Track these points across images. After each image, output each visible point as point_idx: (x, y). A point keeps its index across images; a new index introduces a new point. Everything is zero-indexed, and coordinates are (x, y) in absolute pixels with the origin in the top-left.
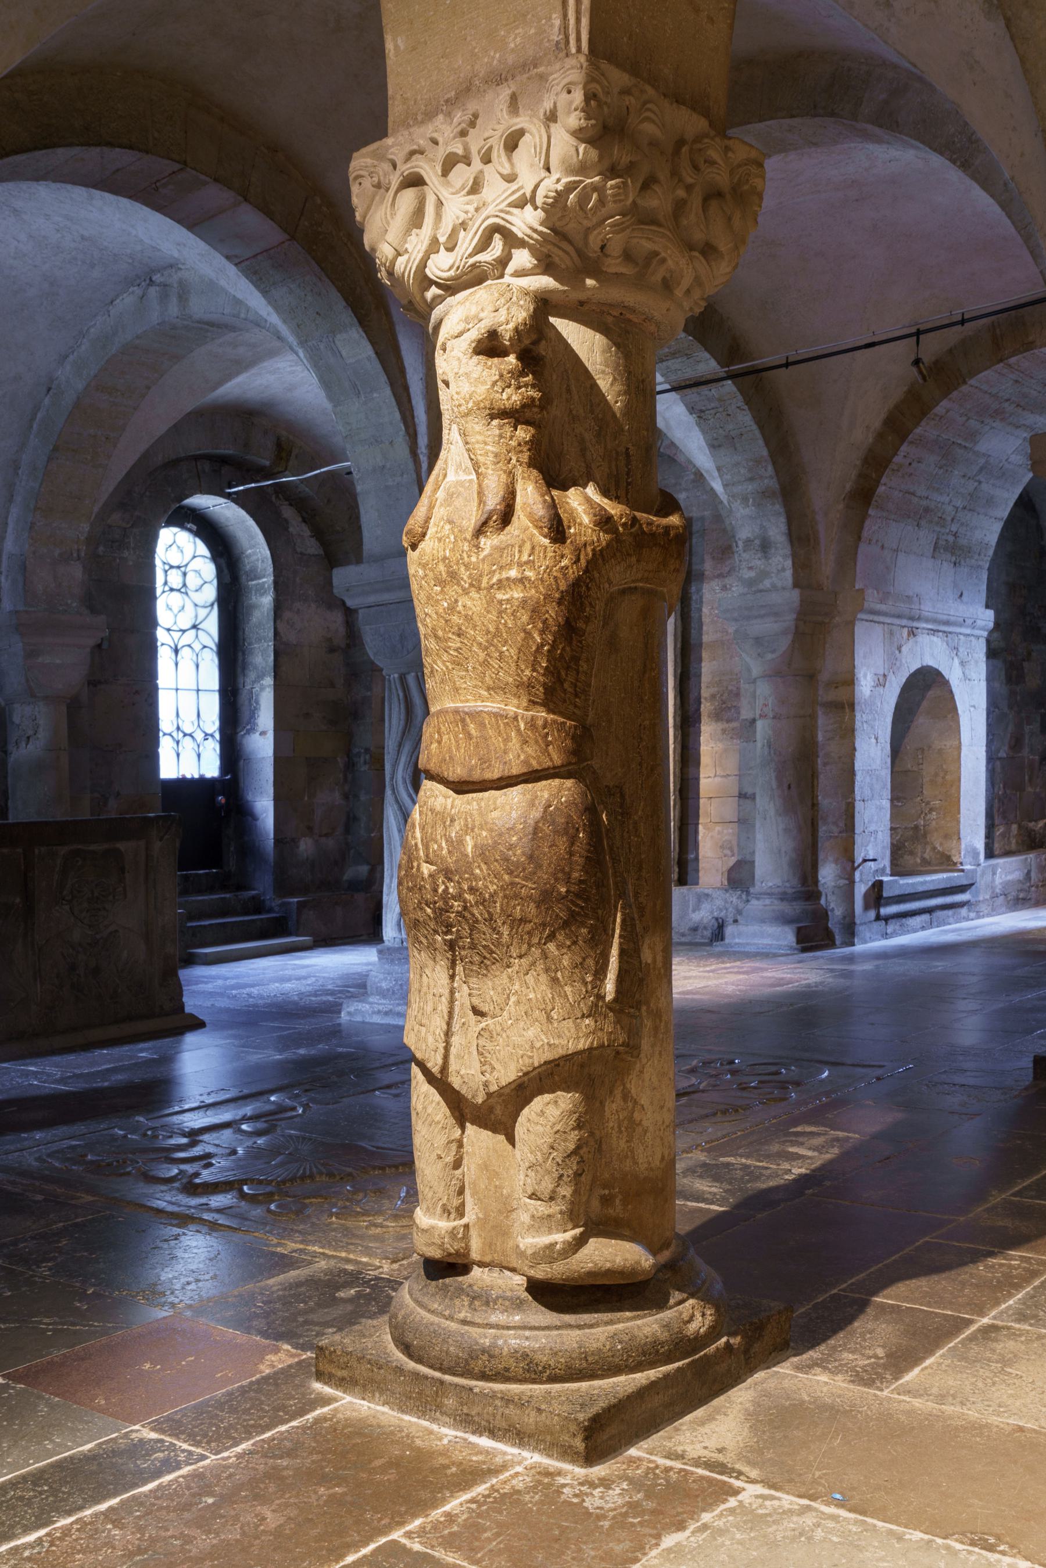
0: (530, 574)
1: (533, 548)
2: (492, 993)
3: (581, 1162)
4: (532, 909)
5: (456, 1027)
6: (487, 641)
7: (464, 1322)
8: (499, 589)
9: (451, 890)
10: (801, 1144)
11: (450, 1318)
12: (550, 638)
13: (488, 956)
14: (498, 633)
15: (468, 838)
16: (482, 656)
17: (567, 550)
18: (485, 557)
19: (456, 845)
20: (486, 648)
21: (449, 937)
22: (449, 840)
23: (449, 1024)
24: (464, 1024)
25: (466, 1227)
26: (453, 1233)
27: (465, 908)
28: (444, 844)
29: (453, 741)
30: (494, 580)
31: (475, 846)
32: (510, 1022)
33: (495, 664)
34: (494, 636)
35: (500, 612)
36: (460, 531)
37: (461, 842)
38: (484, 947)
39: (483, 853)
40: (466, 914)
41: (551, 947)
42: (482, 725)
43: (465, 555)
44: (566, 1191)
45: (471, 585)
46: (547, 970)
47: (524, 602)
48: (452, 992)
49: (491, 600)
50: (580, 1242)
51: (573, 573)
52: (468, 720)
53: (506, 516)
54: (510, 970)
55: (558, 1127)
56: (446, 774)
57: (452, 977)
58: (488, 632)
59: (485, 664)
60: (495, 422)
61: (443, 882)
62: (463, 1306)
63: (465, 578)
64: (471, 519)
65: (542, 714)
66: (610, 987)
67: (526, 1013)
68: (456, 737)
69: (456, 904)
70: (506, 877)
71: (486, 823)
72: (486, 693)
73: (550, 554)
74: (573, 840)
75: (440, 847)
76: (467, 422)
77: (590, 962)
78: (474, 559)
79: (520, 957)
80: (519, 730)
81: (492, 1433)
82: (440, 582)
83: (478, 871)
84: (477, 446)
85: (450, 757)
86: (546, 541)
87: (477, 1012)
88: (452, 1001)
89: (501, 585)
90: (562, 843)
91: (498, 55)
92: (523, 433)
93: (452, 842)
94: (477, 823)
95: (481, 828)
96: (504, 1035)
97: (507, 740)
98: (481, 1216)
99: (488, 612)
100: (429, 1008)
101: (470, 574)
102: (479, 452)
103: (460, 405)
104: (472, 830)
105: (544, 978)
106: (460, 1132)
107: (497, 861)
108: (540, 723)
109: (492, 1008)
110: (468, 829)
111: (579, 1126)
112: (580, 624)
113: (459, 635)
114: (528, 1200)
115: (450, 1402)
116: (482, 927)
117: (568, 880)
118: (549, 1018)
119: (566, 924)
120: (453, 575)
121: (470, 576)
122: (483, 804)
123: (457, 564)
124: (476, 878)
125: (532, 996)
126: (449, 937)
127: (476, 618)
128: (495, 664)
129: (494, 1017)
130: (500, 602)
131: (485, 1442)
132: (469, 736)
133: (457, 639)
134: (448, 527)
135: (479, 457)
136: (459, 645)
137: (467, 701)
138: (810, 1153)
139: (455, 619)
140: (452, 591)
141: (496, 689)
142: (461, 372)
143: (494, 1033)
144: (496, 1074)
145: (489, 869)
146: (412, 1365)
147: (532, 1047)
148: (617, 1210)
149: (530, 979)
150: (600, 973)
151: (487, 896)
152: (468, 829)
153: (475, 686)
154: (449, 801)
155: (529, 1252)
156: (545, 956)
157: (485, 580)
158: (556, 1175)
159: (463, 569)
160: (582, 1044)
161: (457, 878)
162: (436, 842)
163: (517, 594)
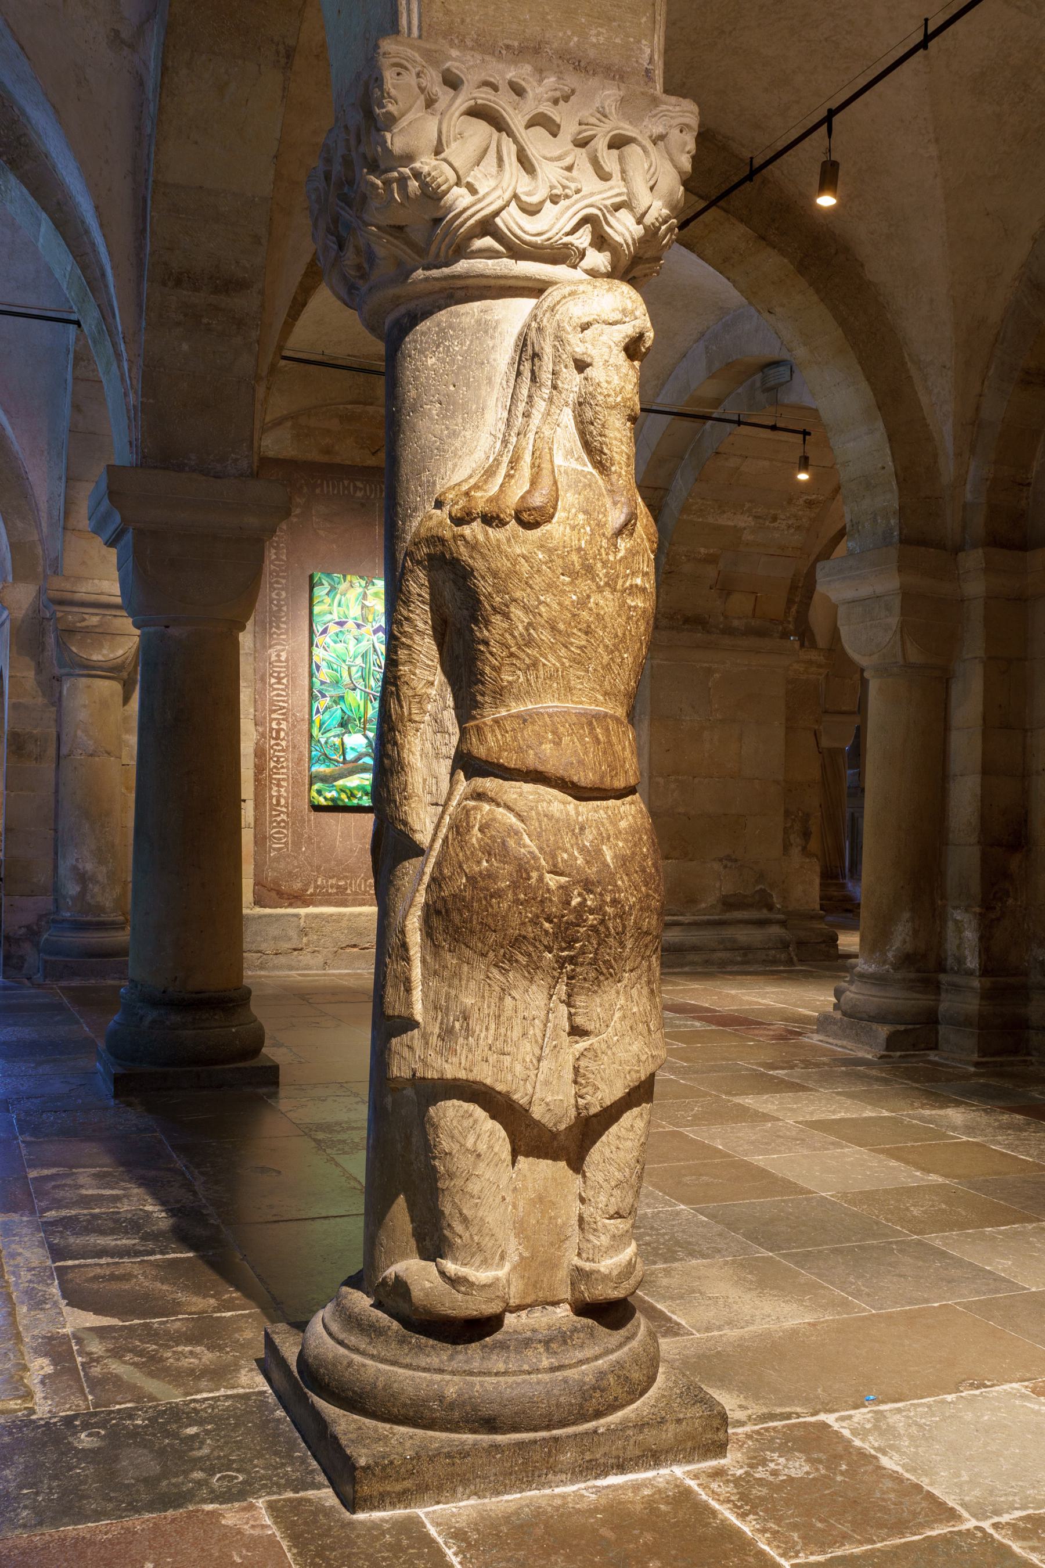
2: (599, 1010)
6: (614, 645)
7: (553, 1369)
8: (629, 594)
9: (589, 903)
11: (538, 1371)
13: (605, 971)
15: (604, 847)
16: (606, 659)
18: (622, 558)
19: (593, 855)
20: (612, 652)
22: (582, 850)
24: (555, 1047)
27: (602, 922)
28: (576, 853)
29: (577, 744)
30: (628, 584)
31: (615, 856)
32: (615, 1038)
34: (621, 641)
36: (598, 525)
37: (599, 852)
38: (604, 962)
40: (602, 929)
43: (603, 550)
45: (607, 584)
54: (619, 985)
56: (575, 779)
58: (616, 636)
59: (607, 668)
61: (580, 895)
63: (601, 575)
67: (631, 1028)
69: (591, 917)
70: (643, 889)
71: (620, 832)
72: (601, 698)
76: (610, 415)
79: (631, 971)
81: (621, 1468)
82: (574, 575)
83: (619, 883)
84: (614, 442)
85: (579, 762)
91: (576, 39)
93: (589, 851)
94: (611, 833)
95: (617, 838)
96: (609, 1052)
98: (526, 1254)
99: (619, 616)
101: (608, 573)
102: (615, 449)
103: (609, 395)
104: (608, 839)
107: (637, 872)
109: (598, 1026)
110: (605, 838)
113: (586, 633)
114: (607, 1221)
115: (568, 1457)
116: (611, 941)
120: (589, 570)
121: (607, 574)
123: (595, 558)
124: (620, 891)
125: (635, 1010)
128: (615, 668)
130: (630, 607)
131: (614, 1480)
132: (597, 741)
133: (583, 636)
135: (615, 455)
136: (584, 643)
137: (581, 703)
139: (585, 614)
140: (585, 585)
142: (611, 362)
143: (599, 1052)
144: (599, 1095)
145: (630, 880)
147: (639, 1061)
151: (627, 908)
152: (605, 838)
153: (593, 689)
155: (615, 1273)
157: (620, 582)
159: (599, 565)
161: (599, 890)
162: (566, 851)
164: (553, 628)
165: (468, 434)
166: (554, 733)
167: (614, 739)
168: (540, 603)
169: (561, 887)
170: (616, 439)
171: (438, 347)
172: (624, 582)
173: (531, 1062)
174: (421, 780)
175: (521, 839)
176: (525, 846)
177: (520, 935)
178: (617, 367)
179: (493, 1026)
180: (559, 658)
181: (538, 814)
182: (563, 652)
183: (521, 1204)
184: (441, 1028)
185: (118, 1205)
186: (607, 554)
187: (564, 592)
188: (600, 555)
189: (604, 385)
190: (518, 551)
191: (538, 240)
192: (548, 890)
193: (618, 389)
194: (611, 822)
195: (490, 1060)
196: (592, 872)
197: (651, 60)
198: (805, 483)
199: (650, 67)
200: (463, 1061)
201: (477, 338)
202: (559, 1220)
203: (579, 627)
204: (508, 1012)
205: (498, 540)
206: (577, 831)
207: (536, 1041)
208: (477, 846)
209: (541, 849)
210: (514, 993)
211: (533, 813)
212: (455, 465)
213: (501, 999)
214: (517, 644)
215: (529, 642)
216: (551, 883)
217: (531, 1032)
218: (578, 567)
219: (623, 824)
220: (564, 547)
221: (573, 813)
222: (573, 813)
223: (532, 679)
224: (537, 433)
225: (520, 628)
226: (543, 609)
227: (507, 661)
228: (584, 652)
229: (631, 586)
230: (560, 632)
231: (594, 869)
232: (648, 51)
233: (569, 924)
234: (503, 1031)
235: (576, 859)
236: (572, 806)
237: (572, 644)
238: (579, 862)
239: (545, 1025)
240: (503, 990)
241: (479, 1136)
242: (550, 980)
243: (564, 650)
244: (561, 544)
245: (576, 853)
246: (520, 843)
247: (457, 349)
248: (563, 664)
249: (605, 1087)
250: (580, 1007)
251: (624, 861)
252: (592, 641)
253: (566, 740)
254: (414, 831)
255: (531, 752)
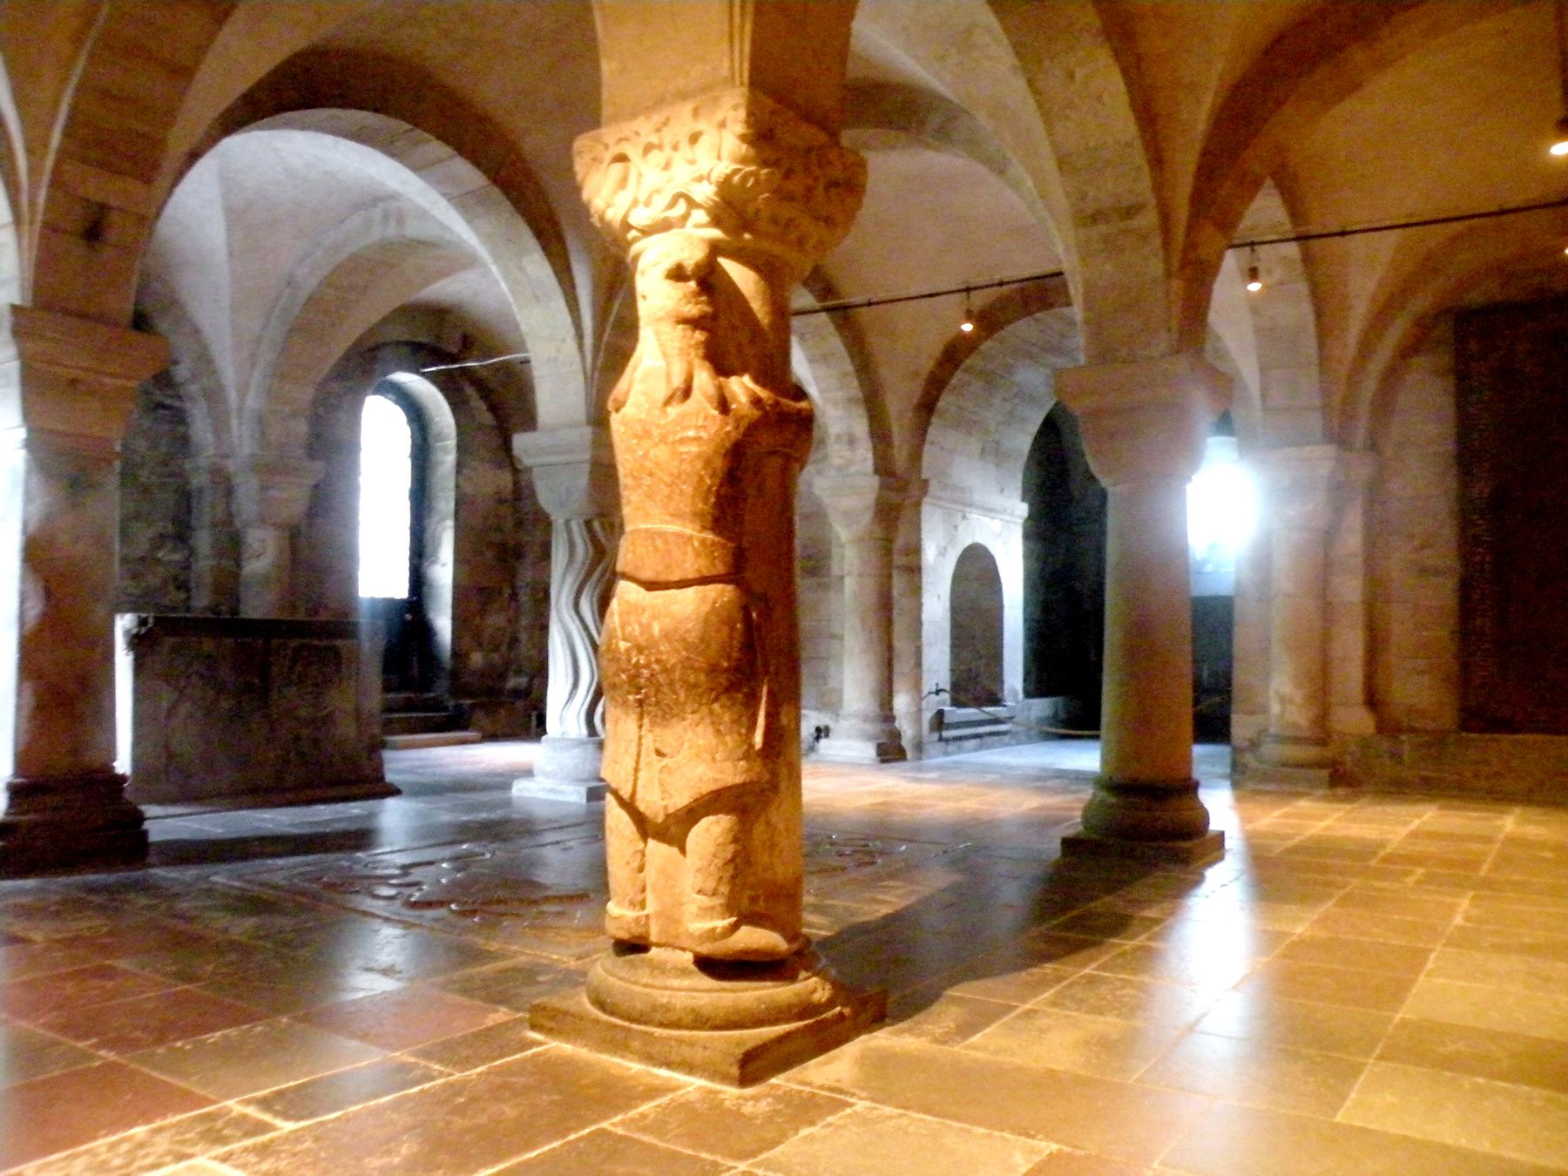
0: (703, 434)
1: (706, 417)
3: (736, 868)
4: (702, 677)
5: (642, 765)
7: (646, 986)
10: (886, 893)
11: (636, 983)
12: (717, 481)
14: (679, 476)
16: (667, 491)
17: (730, 419)
21: (639, 697)
22: (640, 624)
23: (637, 762)
25: (647, 916)
26: (637, 920)
27: (652, 675)
31: (661, 630)
33: (677, 498)
37: (649, 626)
39: (667, 636)
41: (716, 706)
42: (666, 542)
44: (725, 889)
45: (660, 441)
46: (713, 723)
47: (699, 455)
48: (640, 738)
49: (674, 453)
50: (735, 927)
51: (735, 436)
53: (687, 392)
54: (684, 723)
55: (719, 841)
57: (640, 727)
59: (669, 497)
60: (681, 326)
64: (662, 393)
65: (710, 536)
66: (758, 739)
70: (684, 653)
73: (718, 422)
74: (733, 629)
75: (634, 630)
77: (744, 719)
80: (693, 546)
81: (668, 1065)
82: (636, 436)
86: (716, 413)
87: (659, 753)
88: (640, 745)
89: (683, 441)
90: (725, 631)
92: (700, 336)
95: (665, 616)
97: (685, 553)
100: (622, 750)
105: (710, 729)
106: (643, 845)
108: (709, 542)
110: (655, 617)
111: (735, 840)
112: (739, 473)
115: (636, 1044)
117: (729, 658)
118: (714, 759)
119: (727, 690)
124: (660, 653)
126: (639, 697)
129: (672, 757)
130: (682, 453)
131: (663, 1072)
137: (655, 523)
138: (894, 900)
140: (646, 444)
141: (676, 516)
146: (604, 1017)
148: (761, 906)
149: (700, 729)
150: (752, 727)
152: (655, 617)
155: (697, 933)
156: (711, 713)
158: (717, 877)
159: (654, 428)
160: (738, 780)
163: (694, 449)
192: (620, 653)
196: (642, 641)
198: (1260, 292)
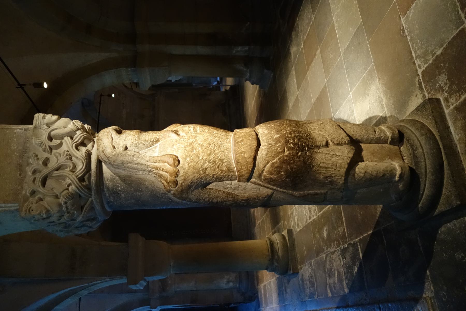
2: (320, 138)
6: (212, 136)
9: (292, 141)
11: (423, 153)
13: (309, 136)
15: (274, 137)
16: (217, 138)
20: (214, 136)
22: (276, 144)
24: (332, 150)
27: (297, 137)
28: (277, 146)
29: (244, 146)
31: (277, 134)
33: (219, 135)
34: (211, 134)
35: (204, 132)
36: (177, 142)
37: (276, 139)
38: (307, 137)
40: (298, 137)
43: (184, 140)
45: (194, 138)
52: (237, 141)
54: (312, 132)
56: (255, 147)
58: (209, 135)
59: (219, 138)
61: (290, 144)
62: (418, 152)
67: (323, 128)
68: (243, 145)
69: (296, 141)
70: (285, 125)
71: (269, 133)
76: (141, 139)
78: (186, 137)
79: (307, 129)
83: (284, 132)
84: (150, 137)
85: (250, 146)
91: (16, 153)
93: (276, 142)
94: (269, 135)
95: (271, 134)
96: (331, 135)
98: (388, 157)
99: (203, 135)
101: (191, 138)
103: (136, 139)
104: (271, 136)
107: (280, 128)
109: (325, 138)
113: (210, 144)
114: (377, 134)
116: (301, 135)
120: (191, 144)
122: (263, 136)
123: (187, 142)
125: (318, 127)
127: (205, 138)
128: (219, 135)
132: (242, 140)
134: (174, 147)
135: (153, 137)
136: (213, 145)
137: (231, 145)
139: (205, 145)
140: (196, 145)
142: (125, 139)
143: (332, 138)
144: (344, 137)
145: (283, 129)
146: (445, 162)
147: (332, 126)
151: (291, 130)
154: (263, 148)
155: (391, 132)
157: (193, 135)
159: (189, 141)
161: (288, 139)
162: (277, 149)
164: (210, 155)
165: (147, 183)
166: (241, 153)
167: (241, 135)
168: (202, 159)
169: (288, 150)
170: (149, 137)
171: (119, 194)
172: (193, 133)
173: (338, 157)
174: (253, 194)
175: (275, 162)
176: (277, 161)
177: (303, 162)
178: (126, 137)
179: (329, 169)
180: (218, 153)
181: (267, 158)
182: (216, 151)
183: (375, 159)
184: (329, 185)
185: (341, 272)
186: (185, 139)
187: (198, 152)
188: (186, 141)
189: (132, 141)
190: (187, 166)
191: (85, 163)
192: (289, 154)
193: (133, 136)
194: (266, 135)
195: (339, 169)
196: (283, 141)
197: (21, 129)
199: (23, 129)
200: (339, 178)
201: (116, 182)
202: (378, 148)
203: (208, 147)
204: (324, 165)
205: (183, 172)
206: (270, 146)
207: (332, 156)
208: (277, 176)
209: (277, 156)
210: (319, 163)
211: (266, 159)
212: (157, 187)
213: (321, 167)
214: (215, 166)
215: (214, 162)
216: (287, 153)
217: (329, 158)
218: (190, 148)
219: (266, 132)
220: (185, 152)
221: (265, 147)
222: (265, 147)
223: (225, 161)
224: (148, 162)
225: (210, 165)
226: (204, 158)
227: (220, 169)
228: (216, 145)
229: (194, 131)
230: (211, 152)
231: (282, 140)
232: (18, 130)
233: (298, 147)
234: (330, 166)
235: (279, 146)
236: (263, 147)
237: (214, 149)
238: (280, 145)
239: (327, 154)
240: (318, 166)
241: (360, 172)
242: (314, 153)
243: (216, 151)
244: (184, 153)
245: (277, 146)
246: (276, 163)
247: (120, 188)
248: (220, 151)
249: (341, 136)
250: (320, 143)
251: (278, 132)
252: (212, 143)
253: (243, 150)
254: (268, 195)
255: (248, 160)
